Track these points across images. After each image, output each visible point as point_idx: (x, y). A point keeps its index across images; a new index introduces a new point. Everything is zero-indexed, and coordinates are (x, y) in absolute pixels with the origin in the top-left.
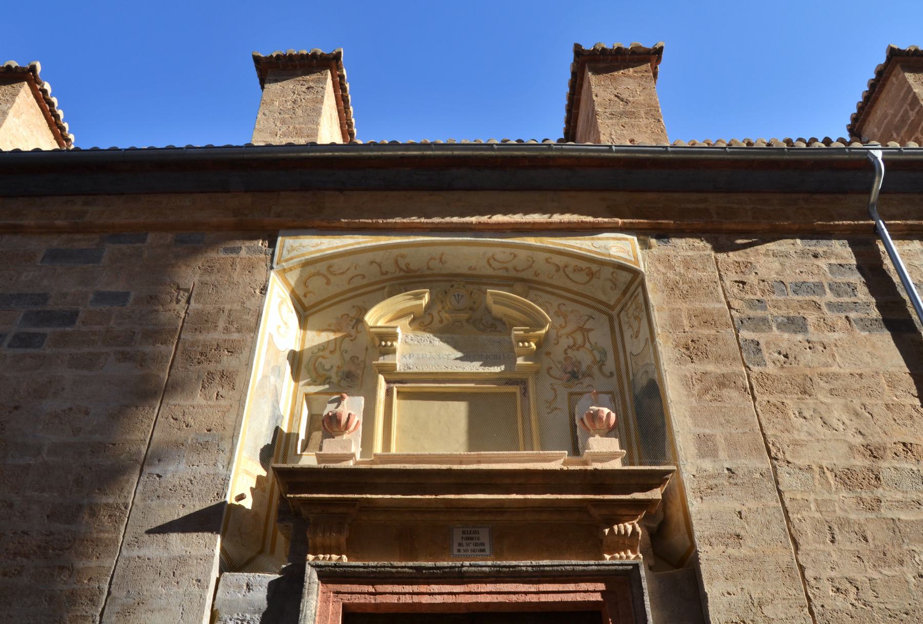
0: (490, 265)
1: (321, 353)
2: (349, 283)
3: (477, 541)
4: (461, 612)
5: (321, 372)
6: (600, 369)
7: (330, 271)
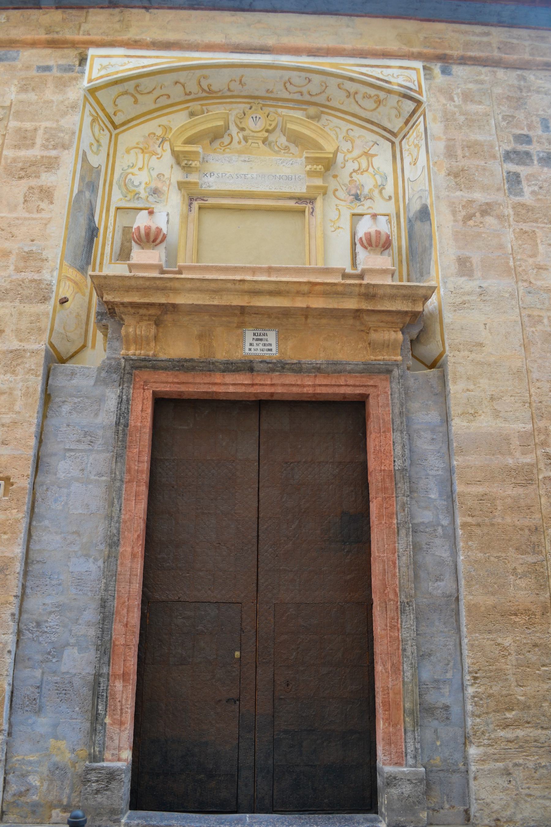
0: (286, 89)
1: (130, 170)
2: (155, 102)
4: (251, 399)
5: (131, 188)
6: (381, 192)
7: (137, 90)
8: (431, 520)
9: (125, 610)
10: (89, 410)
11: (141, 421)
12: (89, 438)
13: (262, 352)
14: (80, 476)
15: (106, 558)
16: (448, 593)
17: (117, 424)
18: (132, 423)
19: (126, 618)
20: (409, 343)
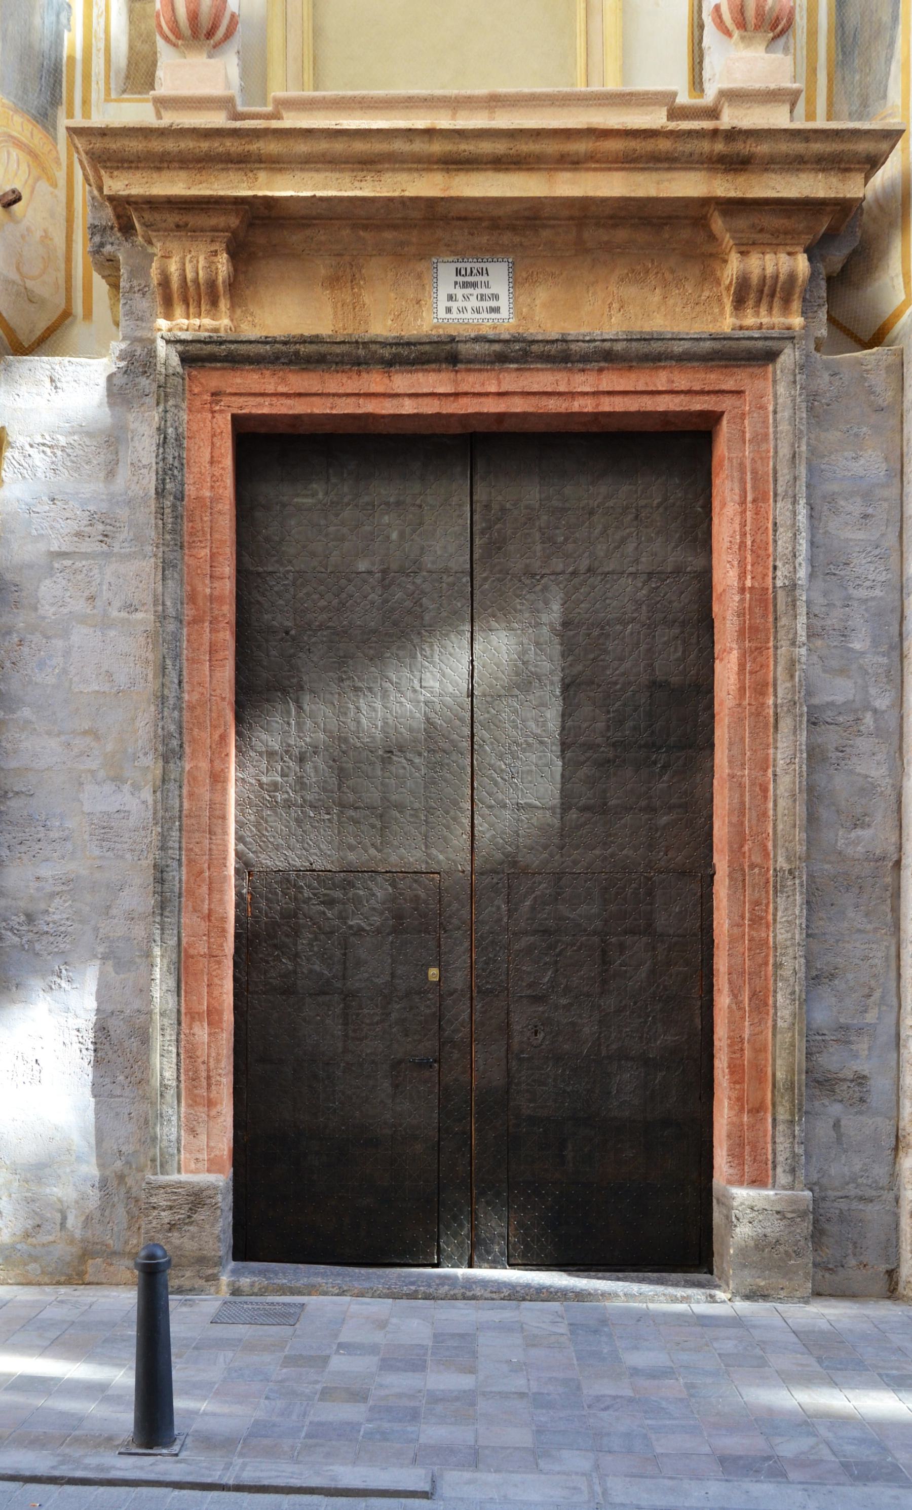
3: (484, 291)
4: (451, 431)
8: (851, 697)
9: (205, 889)
10: (95, 462)
11: (212, 487)
12: (101, 527)
13: (476, 316)
14: (88, 611)
15: (159, 783)
16: (878, 852)
17: (160, 493)
18: (190, 490)
19: (207, 902)
20: (823, 284)
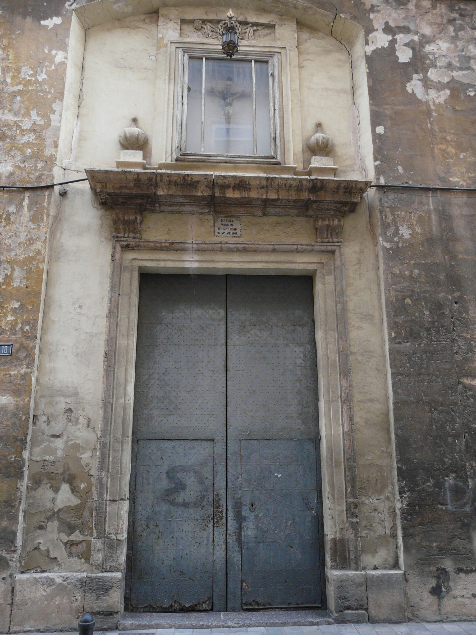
3: (231, 227)
